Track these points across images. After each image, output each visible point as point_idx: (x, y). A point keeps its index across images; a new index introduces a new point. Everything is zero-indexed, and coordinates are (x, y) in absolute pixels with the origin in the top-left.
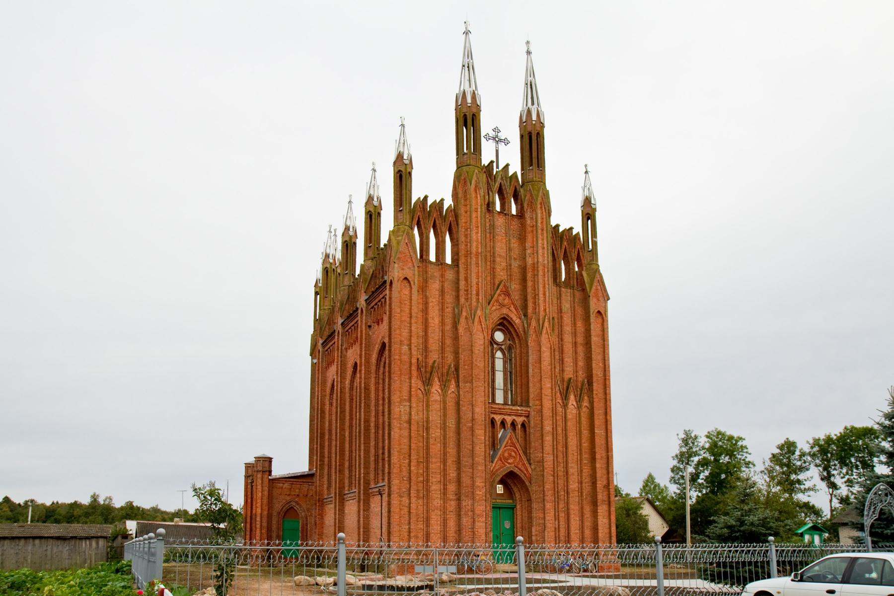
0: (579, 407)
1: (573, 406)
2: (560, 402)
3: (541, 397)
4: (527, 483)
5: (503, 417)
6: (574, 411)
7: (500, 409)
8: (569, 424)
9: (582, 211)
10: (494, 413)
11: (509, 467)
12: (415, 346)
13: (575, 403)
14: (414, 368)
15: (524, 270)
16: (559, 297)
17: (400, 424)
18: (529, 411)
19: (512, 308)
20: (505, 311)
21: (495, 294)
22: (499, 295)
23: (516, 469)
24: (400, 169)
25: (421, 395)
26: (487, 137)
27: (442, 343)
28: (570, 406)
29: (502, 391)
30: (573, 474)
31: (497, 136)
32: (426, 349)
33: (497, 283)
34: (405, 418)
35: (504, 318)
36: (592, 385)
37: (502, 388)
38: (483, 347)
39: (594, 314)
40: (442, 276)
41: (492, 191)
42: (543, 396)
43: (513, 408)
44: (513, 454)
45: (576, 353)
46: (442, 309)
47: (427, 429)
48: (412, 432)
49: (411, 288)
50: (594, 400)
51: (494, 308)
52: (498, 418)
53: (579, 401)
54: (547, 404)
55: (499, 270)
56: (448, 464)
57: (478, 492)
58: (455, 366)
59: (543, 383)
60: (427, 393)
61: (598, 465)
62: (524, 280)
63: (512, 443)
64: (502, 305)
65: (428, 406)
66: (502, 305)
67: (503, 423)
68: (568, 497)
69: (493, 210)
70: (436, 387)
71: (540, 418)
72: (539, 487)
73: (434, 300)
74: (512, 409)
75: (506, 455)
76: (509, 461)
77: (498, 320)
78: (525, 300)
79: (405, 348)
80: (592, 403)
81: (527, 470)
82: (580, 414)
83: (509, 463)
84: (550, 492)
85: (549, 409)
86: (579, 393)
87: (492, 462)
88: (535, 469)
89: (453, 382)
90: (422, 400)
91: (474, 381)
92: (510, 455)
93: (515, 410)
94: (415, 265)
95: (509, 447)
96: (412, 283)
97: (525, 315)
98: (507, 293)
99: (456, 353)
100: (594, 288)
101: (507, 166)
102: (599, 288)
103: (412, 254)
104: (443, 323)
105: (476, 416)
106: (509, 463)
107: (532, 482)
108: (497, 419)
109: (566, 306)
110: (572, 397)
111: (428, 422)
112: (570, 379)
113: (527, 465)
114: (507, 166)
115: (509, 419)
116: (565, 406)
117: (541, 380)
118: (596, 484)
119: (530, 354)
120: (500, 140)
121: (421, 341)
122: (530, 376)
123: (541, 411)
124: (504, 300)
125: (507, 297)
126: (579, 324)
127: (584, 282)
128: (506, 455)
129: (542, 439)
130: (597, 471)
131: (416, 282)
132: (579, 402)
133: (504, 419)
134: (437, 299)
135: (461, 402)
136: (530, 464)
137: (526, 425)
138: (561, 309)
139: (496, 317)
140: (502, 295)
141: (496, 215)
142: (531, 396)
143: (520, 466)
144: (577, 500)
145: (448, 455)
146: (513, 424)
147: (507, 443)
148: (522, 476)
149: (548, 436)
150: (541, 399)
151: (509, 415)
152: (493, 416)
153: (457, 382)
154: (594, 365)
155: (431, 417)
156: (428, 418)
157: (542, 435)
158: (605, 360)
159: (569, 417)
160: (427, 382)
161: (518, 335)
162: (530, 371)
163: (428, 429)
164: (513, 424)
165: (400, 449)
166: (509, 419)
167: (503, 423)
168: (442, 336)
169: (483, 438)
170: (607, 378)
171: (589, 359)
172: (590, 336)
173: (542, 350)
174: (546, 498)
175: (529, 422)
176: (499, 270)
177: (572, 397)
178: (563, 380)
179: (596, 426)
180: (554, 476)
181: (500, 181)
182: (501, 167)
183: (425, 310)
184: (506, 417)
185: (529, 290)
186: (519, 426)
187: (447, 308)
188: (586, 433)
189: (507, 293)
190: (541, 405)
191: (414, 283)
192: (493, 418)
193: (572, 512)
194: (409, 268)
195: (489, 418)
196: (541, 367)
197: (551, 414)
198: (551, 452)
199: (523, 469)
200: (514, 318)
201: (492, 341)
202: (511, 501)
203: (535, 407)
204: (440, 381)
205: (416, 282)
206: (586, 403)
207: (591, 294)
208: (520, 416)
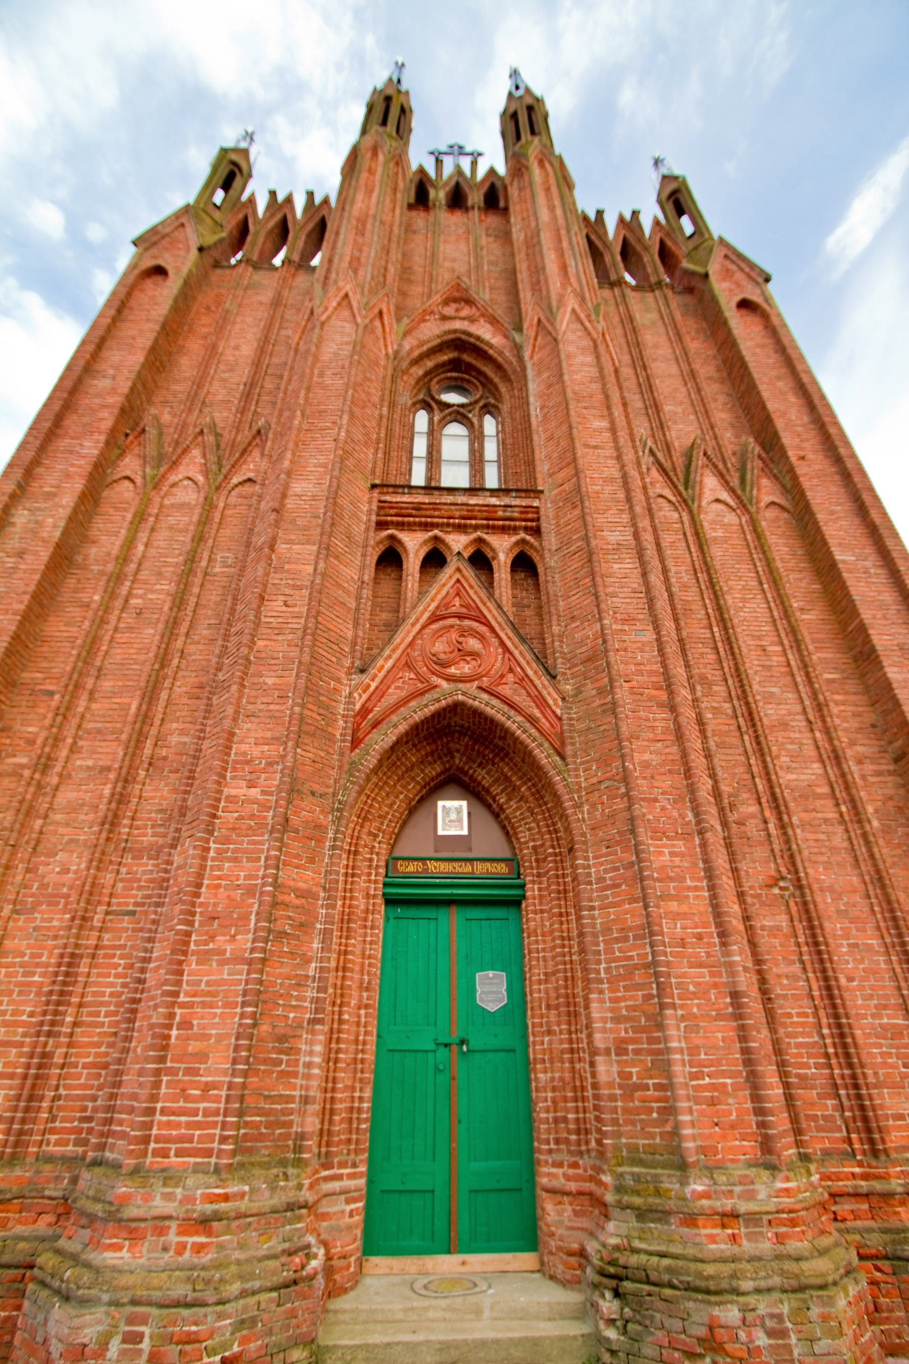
4: (543, 755)
23: (485, 696)
63: (467, 606)
68: (782, 827)
72: (604, 762)
76: (453, 670)
81: (540, 701)
83: (450, 679)
84: (667, 783)
88: (578, 691)
107: (569, 750)
113: (541, 682)
143: (505, 690)
148: (514, 723)
149: (620, 561)
161: (499, 367)
174: (639, 809)
180: (673, 709)
193: (825, 903)
198: (643, 615)
199: (521, 699)
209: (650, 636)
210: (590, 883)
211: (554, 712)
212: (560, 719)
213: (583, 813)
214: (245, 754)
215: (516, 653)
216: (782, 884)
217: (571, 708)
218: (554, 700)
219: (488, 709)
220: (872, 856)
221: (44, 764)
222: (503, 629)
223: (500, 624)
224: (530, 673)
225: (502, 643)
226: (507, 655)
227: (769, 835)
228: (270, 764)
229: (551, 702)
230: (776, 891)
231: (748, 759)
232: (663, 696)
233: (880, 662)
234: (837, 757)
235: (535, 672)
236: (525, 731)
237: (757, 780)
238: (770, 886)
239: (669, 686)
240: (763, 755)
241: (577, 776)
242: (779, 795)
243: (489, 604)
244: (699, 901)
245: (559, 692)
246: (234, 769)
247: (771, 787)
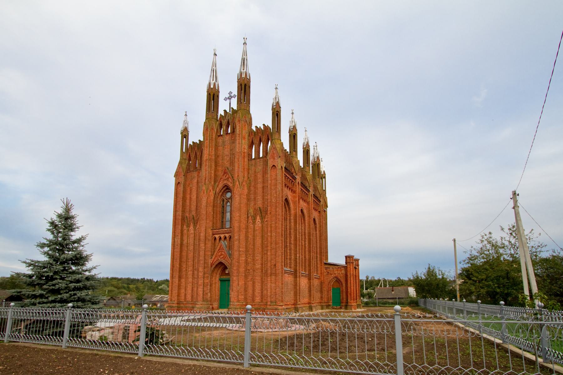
5: (219, 235)
6: (260, 225)
20: (225, 182)
30: (258, 260)
51: (221, 182)
52: (217, 236)
53: (262, 218)
70: (192, 228)
77: (224, 187)
82: (262, 226)
83: (220, 258)
84: (236, 271)
85: (237, 227)
87: (211, 258)
110: (258, 217)
115: (222, 236)
130: (268, 257)
139: (221, 185)
144: (260, 274)
146: (225, 238)
156: (187, 242)
160: (188, 226)
164: (225, 238)
166: (222, 236)
167: (220, 238)
177: (258, 217)
178: (255, 209)
221: (186, 270)
244: (237, 283)
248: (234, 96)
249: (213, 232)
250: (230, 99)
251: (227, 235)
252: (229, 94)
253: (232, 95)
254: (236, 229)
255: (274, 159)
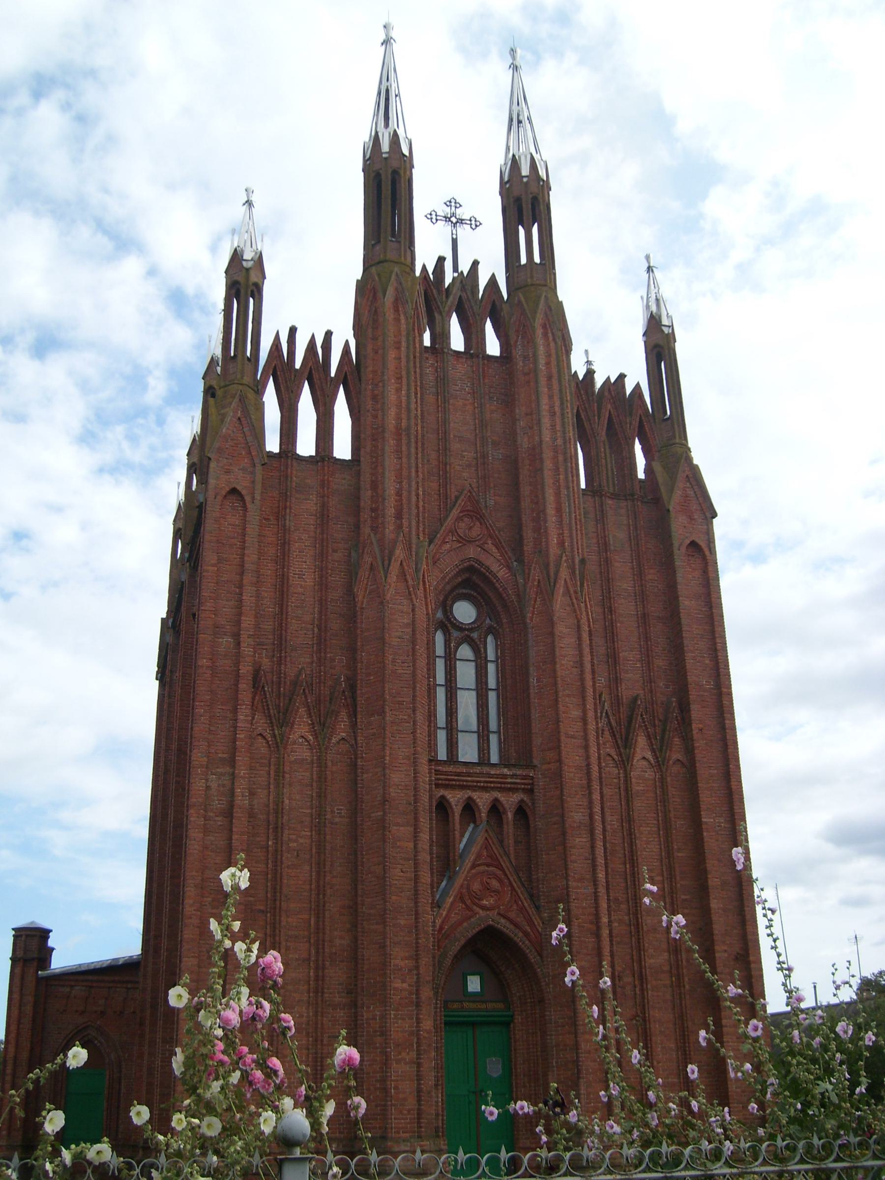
0: (659, 764)
1: (645, 763)
2: (613, 753)
3: (559, 741)
4: (533, 957)
6: (649, 774)
7: (459, 774)
8: (638, 804)
9: (645, 342)
10: (446, 787)
11: (483, 917)
12: (249, 636)
13: (649, 755)
14: (245, 686)
15: (513, 464)
16: (601, 519)
17: (206, 818)
18: (532, 778)
19: (490, 546)
20: (472, 552)
21: (447, 517)
22: (459, 519)
24: (236, 278)
25: (264, 750)
26: (432, 217)
27: (319, 630)
28: (637, 762)
29: (476, 735)
31: (454, 215)
32: (280, 644)
33: (453, 493)
34: (218, 803)
35: (471, 569)
36: (689, 711)
37: (475, 728)
38: (409, 630)
39: (683, 549)
40: (323, 484)
41: (440, 313)
42: (563, 738)
43: (492, 772)
44: (495, 884)
45: (647, 639)
46: (322, 555)
47: (276, 828)
48: (235, 837)
49: (245, 507)
50: (696, 745)
51: (448, 546)
52: (456, 799)
53: (659, 748)
54: (572, 757)
55: (457, 468)
56: (327, 914)
57: (398, 984)
58: (348, 679)
59: (561, 708)
60: (278, 745)
61: (714, 904)
62: (515, 484)
64: (465, 541)
65: (280, 774)
66: (465, 541)
67: (469, 808)
68: (642, 990)
69: (442, 349)
71: (558, 792)
73: (305, 536)
74: (489, 775)
75: (476, 886)
78: (518, 527)
79: (226, 641)
80: (690, 751)
81: (530, 922)
82: (662, 780)
86: (658, 730)
89: (344, 715)
90: (266, 761)
91: (387, 709)
92: (487, 888)
93: (497, 776)
94: (257, 461)
95: (482, 868)
96: (248, 499)
97: (520, 560)
98: (475, 513)
99: (352, 650)
100: (678, 494)
101: (475, 264)
102: (690, 492)
103: (250, 439)
104: (323, 585)
105: (393, 792)
106: (483, 908)
108: (453, 801)
109: (618, 535)
110: (641, 741)
111: (278, 811)
112: (635, 699)
113: (532, 911)
114: (475, 264)
115: (483, 800)
116: (624, 762)
117: (557, 700)
118: (714, 952)
119: (530, 643)
120: (461, 221)
121: (268, 626)
122: (532, 696)
123: (558, 776)
124: (470, 528)
125: (478, 523)
126: (652, 575)
127: (657, 484)
128: (476, 886)
129: (564, 844)
130: (714, 918)
131: (258, 497)
132: (661, 751)
133: (470, 798)
134: (312, 534)
135: (359, 762)
136: (537, 908)
137: (528, 811)
138: (606, 544)
140: (466, 519)
141: (450, 358)
142: (537, 741)
144: (668, 996)
145: (329, 891)
146: (496, 809)
147: (479, 856)
148: (518, 937)
150: (559, 747)
151: (485, 789)
152: (442, 792)
153: (353, 714)
154: (689, 662)
155: (287, 802)
156: (279, 803)
157: (564, 834)
158: (716, 650)
159: (637, 787)
162: (533, 681)
163: (278, 830)
164: (496, 809)
165: (202, 880)
167: (469, 808)
168: (320, 612)
169: (411, 845)
170: (724, 690)
171: (677, 649)
172: (676, 598)
173: (557, 633)
175: (533, 804)
176: (457, 468)
177: (641, 741)
178: (617, 701)
179: (703, 806)
181: (459, 294)
182: (465, 267)
183: (283, 559)
184: (475, 795)
185: (526, 504)
186: (510, 815)
187: (334, 551)
188: (680, 825)
189: (475, 513)
190: (560, 761)
191: (253, 498)
192: (443, 797)
194: (244, 470)
195: (431, 797)
196: (555, 671)
197: (585, 782)
200: (495, 568)
201: (448, 624)
202: (501, 1005)
203: (545, 767)
204: (310, 716)
205: (258, 497)
206: (676, 754)
207: (673, 505)
208: (510, 789)
209: (591, 890)
210: (551, 1023)
211: (538, 930)
212: (541, 935)
213: (549, 988)
214: (397, 965)
215: (519, 891)
216: (637, 1018)
217: (546, 928)
218: (538, 923)
219: (505, 930)
220: (681, 1005)
222: (512, 876)
223: (510, 873)
224: (526, 904)
225: (512, 886)
226: (514, 893)
227: (635, 994)
228: (410, 970)
229: (536, 923)
230: (634, 1022)
231: (632, 951)
232: (594, 928)
233: (708, 892)
234: (676, 950)
235: (529, 905)
236: (523, 943)
237: (635, 964)
238: (632, 1020)
239: (597, 922)
240: (640, 950)
241: (548, 968)
242: (644, 974)
243: (504, 858)
245: (541, 918)
246: (395, 974)
247: (641, 968)
248: (475, 224)
249: (437, 772)
250: (455, 225)
251: (510, 801)
252: (448, 204)
253: (464, 213)
254: (572, 776)
255: (691, 518)
